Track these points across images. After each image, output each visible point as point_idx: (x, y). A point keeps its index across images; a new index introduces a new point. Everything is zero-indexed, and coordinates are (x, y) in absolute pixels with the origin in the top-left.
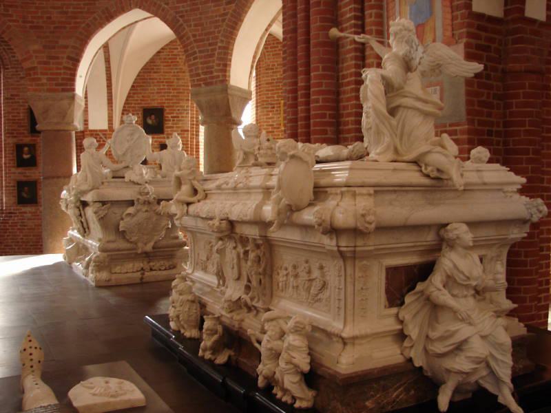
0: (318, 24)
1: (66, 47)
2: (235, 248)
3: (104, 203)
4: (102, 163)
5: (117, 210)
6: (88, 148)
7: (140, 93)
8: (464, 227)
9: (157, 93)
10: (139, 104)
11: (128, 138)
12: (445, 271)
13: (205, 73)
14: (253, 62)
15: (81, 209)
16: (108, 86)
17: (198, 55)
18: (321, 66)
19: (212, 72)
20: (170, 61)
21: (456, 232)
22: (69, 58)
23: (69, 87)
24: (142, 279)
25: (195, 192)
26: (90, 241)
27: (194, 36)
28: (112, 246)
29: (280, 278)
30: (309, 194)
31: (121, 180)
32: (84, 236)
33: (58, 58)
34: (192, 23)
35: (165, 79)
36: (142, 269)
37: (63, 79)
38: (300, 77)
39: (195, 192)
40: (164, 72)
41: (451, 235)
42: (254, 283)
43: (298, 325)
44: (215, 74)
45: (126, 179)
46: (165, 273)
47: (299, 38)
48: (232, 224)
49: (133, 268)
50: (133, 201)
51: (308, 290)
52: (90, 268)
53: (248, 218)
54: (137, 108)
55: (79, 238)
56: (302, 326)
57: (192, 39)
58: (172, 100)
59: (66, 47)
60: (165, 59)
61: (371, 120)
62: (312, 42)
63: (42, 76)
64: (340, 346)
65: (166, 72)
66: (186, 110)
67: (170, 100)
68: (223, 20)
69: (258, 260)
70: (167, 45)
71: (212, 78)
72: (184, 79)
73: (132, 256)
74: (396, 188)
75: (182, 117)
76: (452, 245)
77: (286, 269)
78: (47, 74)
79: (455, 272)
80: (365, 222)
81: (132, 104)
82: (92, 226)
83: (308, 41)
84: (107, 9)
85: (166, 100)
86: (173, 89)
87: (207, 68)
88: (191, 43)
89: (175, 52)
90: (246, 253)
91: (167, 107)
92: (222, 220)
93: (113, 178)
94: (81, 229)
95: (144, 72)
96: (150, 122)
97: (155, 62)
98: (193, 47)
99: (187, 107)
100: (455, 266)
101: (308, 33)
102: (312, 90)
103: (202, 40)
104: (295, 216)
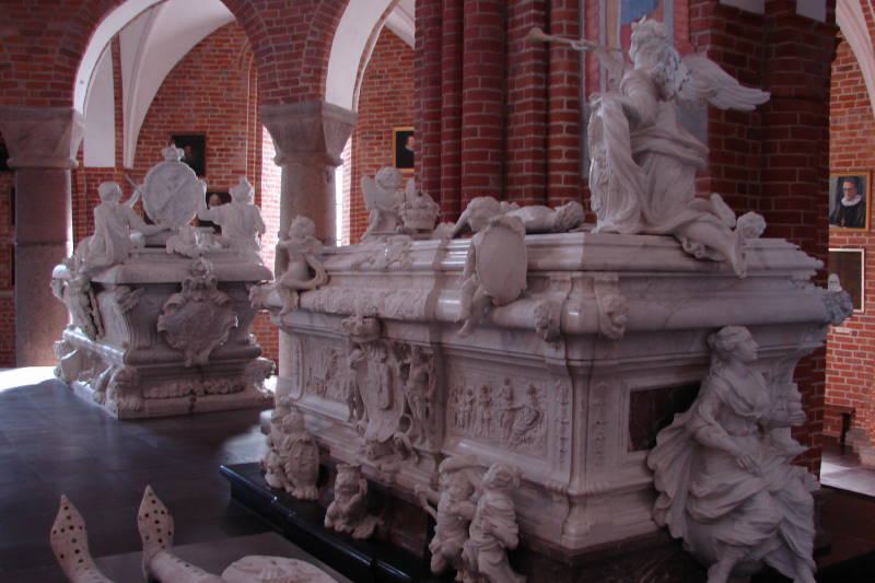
0: (478, 13)
1: (59, 34)
2: (384, 361)
3: (133, 287)
4: (129, 223)
5: (155, 299)
7: (168, 110)
8: (746, 333)
9: (196, 111)
10: (165, 127)
11: (171, 184)
12: (718, 397)
13: (287, 83)
14: (361, 67)
15: (92, 295)
16: (116, 98)
17: (275, 53)
18: (480, 78)
19: (297, 82)
20: (216, 60)
21: (734, 340)
22: (64, 51)
23: (62, 99)
24: (192, 407)
25: (311, 273)
26: (106, 347)
27: (267, 23)
28: (144, 355)
29: (461, 407)
30: (521, 280)
31: (159, 250)
32: (94, 339)
33: (46, 52)
35: (207, 88)
36: (192, 392)
37: (53, 85)
38: (446, 95)
39: (311, 273)
40: (206, 78)
41: (726, 344)
42: (418, 413)
43: (501, 477)
44: (301, 84)
45: (169, 250)
46: (230, 398)
47: (445, 34)
48: (382, 323)
49: (177, 391)
50: (179, 284)
51: (509, 425)
52: (108, 390)
53: (415, 315)
54: (162, 135)
55: (85, 342)
56: (507, 479)
57: (265, 28)
58: (219, 122)
59: (59, 34)
60: (208, 56)
61: (607, 171)
62: (466, 40)
63: (18, 80)
64: (564, 508)
65: (211, 78)
66: (242, 139)
67: (215, 122)
69: (425, 379)
70: (211, 35)
71: (298, 90)
72: (238, 90)
73: (178, 371)
74: (648, 274)
75: (235, 150)
76: (727, 358)
77: (470, 393)
78: (27, 76)
79: (732, 398)
80: (614, 324)
81: (153, 127)
82: (109, 323)
83: (459, 39)
85: (209, 121)
86: (221, 106)
87: (289, 75)
88: (264, 34)
89: (226, 46)
90: (405, 368)
91: (211, 133)
92: (365, 317)
93: (147, 246)
94: (92, 328)
95: (174, 77)
97: (191, 61)
98: (267, 42)
99: (243, 134)
100: (733, 390)
101: (460, 27)
102: (465, 115)
103: (282, 30)
104: (497, 314)
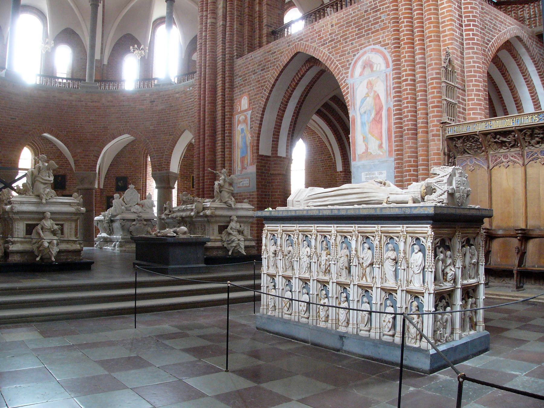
0: (208, 153)
3: (124, 220)
6: (116, 198)
9: (124, 169)
13: (159, 166)
14: (180, 160)
19: (162, 165)
22: (94, 156)
26: (114, 236)
27: (154, 148)
32: (110, 235)
33: (89, 156)
34: (153, 143)
37: (91, 165)
38: (201, 172)
44: (163, 166)
47: (201, 157)
59: (93, 151)
60: (129, 150)
68: (168, 143)
75: (138, 182)
83: (204, 159)
84: (113, 134)
96: (120, 184)
102: (205, 178)
